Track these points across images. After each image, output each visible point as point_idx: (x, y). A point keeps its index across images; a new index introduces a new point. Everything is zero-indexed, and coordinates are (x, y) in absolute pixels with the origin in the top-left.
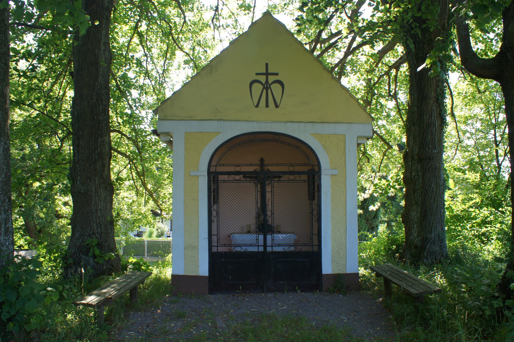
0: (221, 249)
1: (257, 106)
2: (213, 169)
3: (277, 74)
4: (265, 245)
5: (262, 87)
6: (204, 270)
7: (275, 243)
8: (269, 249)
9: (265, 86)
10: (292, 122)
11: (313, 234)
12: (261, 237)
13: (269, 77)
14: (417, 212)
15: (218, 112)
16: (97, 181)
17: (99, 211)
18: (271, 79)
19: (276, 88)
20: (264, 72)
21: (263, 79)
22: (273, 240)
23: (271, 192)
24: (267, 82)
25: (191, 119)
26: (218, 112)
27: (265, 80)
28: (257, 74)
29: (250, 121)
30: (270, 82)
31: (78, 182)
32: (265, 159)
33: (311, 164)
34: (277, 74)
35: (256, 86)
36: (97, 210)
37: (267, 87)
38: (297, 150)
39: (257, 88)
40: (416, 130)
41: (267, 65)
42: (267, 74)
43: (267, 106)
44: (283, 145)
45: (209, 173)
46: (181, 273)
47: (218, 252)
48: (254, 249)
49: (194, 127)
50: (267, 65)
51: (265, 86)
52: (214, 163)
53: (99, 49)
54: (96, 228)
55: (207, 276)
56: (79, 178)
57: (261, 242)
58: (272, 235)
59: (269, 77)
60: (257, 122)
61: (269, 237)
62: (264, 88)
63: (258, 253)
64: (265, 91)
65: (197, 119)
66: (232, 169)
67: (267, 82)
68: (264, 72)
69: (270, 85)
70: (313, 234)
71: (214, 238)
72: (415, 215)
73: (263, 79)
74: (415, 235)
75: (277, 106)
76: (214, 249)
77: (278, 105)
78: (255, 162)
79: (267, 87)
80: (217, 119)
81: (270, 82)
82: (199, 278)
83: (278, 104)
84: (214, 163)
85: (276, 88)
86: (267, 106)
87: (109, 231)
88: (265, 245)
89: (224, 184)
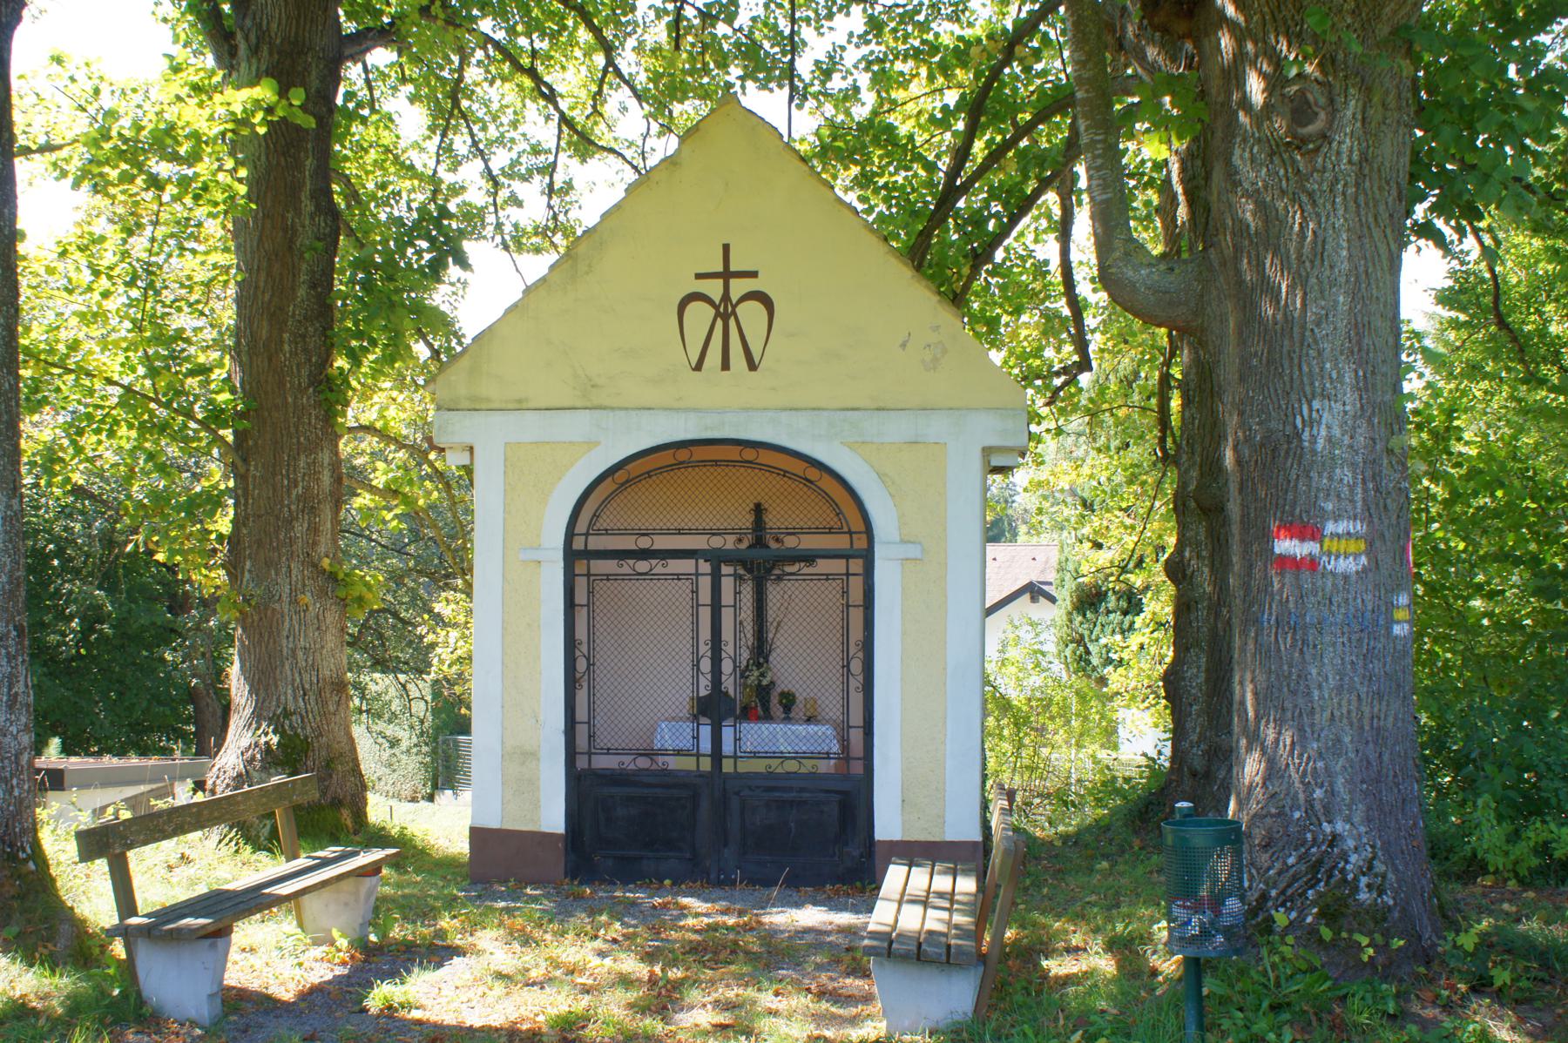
0: (603, 762)
1: (698, 367)
2: (578, 544)
3: (754, 274)
4: (717, 755)
5: (712, 312)
6: (552, 817)
7: (744, 748)
8: (727, 766)
9: (722, 310)
10: (796, 409)
11: (849, 727)
12: (706, 732)
13: (733, 282)
14: (1199, 668)
15: (593, 386)
16: (294, 572)
17: (300, 654)
18: (738, 287)
19: (752, 314)
20: (720, 268)
21: (714, 289)
22: (737, 740)
23: (735, 606)
24: (726, 296)
25: (520, 406)
26: (593, 386)
27: (721, 291)
28: (699, 276)
29: (677, 410)
30: (734, 299)
31: (247, 575)
32: (766, 506)
33: (846, 529)
34: (753, 275)
35: (695, 307)
36: (294, 651)
37: (725, 311)
38: (805, 489)
39: (699, 315)
40: (1194, 419)
41: (726, 248)
42: (727, 275)
43: (726, 365)
44: (767, 474)
45: (572, 556)
46: (494, 824)
47: (590, 769)
48: (688, 764)
49: (529, 427)
50: (726, 248)
51: (722, 310)
52: (581, 526)
53: (298, 212)
54: (290, 698)
55: (561, 835)
56: (248, 564)
57: (706, 745)
58: (735, 726)
59: (733, 282)
60: (695, 410)
61: (727, 734)
62: (718, 314)
63: (701, 775)
64: (719, 323)
65: (537, 406)
66: (628, 543)
67: (726, 296)
68: (720, 268)
69: (734, 307)
70: (849, 727)
71: (582, 732)
72: (1196, 676)
73: (714, 289)
74: (1194, 738)
75: (752, 366)
76: (581, 763)
77: (757, 362)
78: (704, 524)
79: (725, 311)
80: (589, 404)
81: (734, 299)
82: (542, 839)
83: (757, 361)
84: (581, 526)
85: (752, 314)
86: (726, 365)
87: (332, 708)
88: (717, 755)
89: (608, 584)
